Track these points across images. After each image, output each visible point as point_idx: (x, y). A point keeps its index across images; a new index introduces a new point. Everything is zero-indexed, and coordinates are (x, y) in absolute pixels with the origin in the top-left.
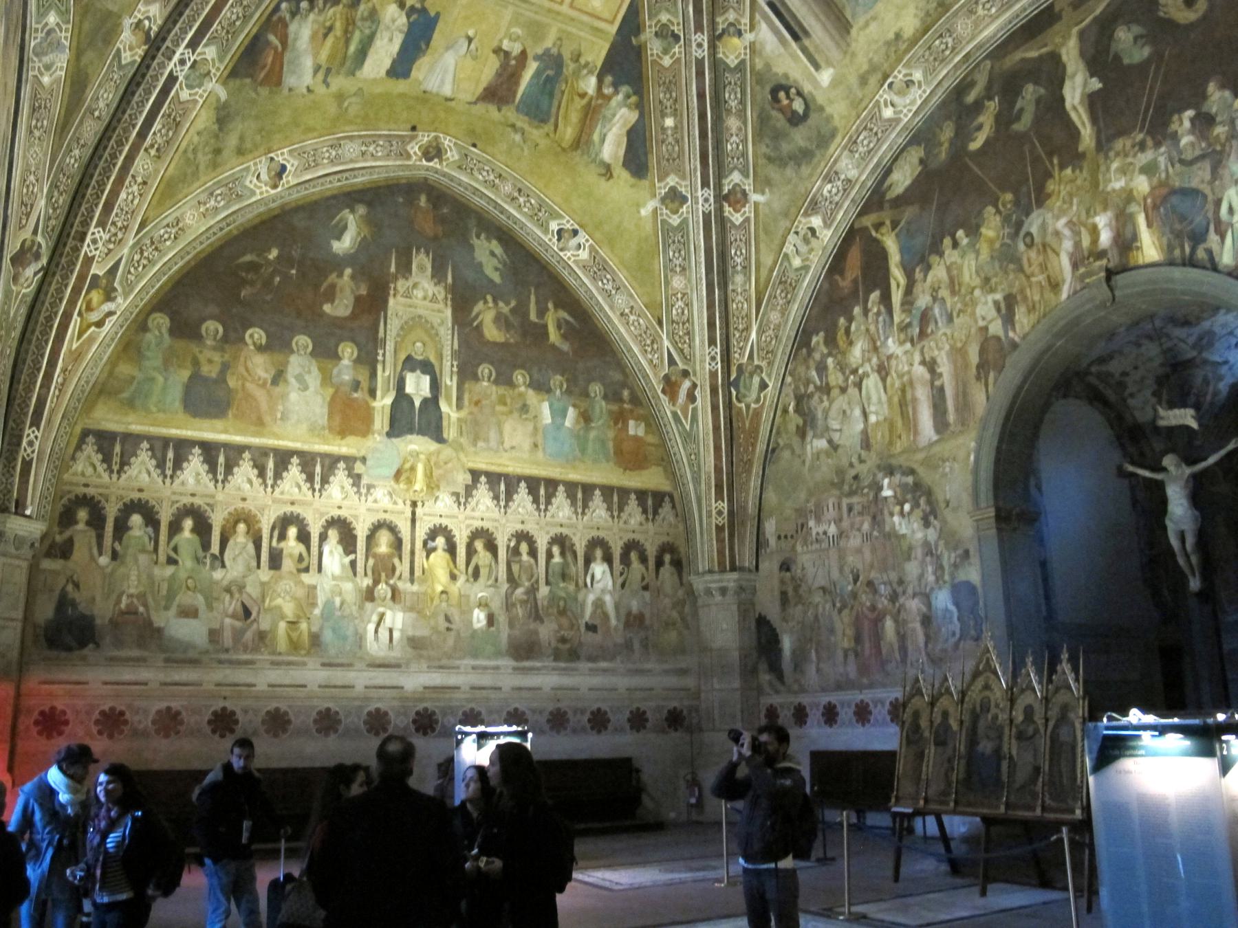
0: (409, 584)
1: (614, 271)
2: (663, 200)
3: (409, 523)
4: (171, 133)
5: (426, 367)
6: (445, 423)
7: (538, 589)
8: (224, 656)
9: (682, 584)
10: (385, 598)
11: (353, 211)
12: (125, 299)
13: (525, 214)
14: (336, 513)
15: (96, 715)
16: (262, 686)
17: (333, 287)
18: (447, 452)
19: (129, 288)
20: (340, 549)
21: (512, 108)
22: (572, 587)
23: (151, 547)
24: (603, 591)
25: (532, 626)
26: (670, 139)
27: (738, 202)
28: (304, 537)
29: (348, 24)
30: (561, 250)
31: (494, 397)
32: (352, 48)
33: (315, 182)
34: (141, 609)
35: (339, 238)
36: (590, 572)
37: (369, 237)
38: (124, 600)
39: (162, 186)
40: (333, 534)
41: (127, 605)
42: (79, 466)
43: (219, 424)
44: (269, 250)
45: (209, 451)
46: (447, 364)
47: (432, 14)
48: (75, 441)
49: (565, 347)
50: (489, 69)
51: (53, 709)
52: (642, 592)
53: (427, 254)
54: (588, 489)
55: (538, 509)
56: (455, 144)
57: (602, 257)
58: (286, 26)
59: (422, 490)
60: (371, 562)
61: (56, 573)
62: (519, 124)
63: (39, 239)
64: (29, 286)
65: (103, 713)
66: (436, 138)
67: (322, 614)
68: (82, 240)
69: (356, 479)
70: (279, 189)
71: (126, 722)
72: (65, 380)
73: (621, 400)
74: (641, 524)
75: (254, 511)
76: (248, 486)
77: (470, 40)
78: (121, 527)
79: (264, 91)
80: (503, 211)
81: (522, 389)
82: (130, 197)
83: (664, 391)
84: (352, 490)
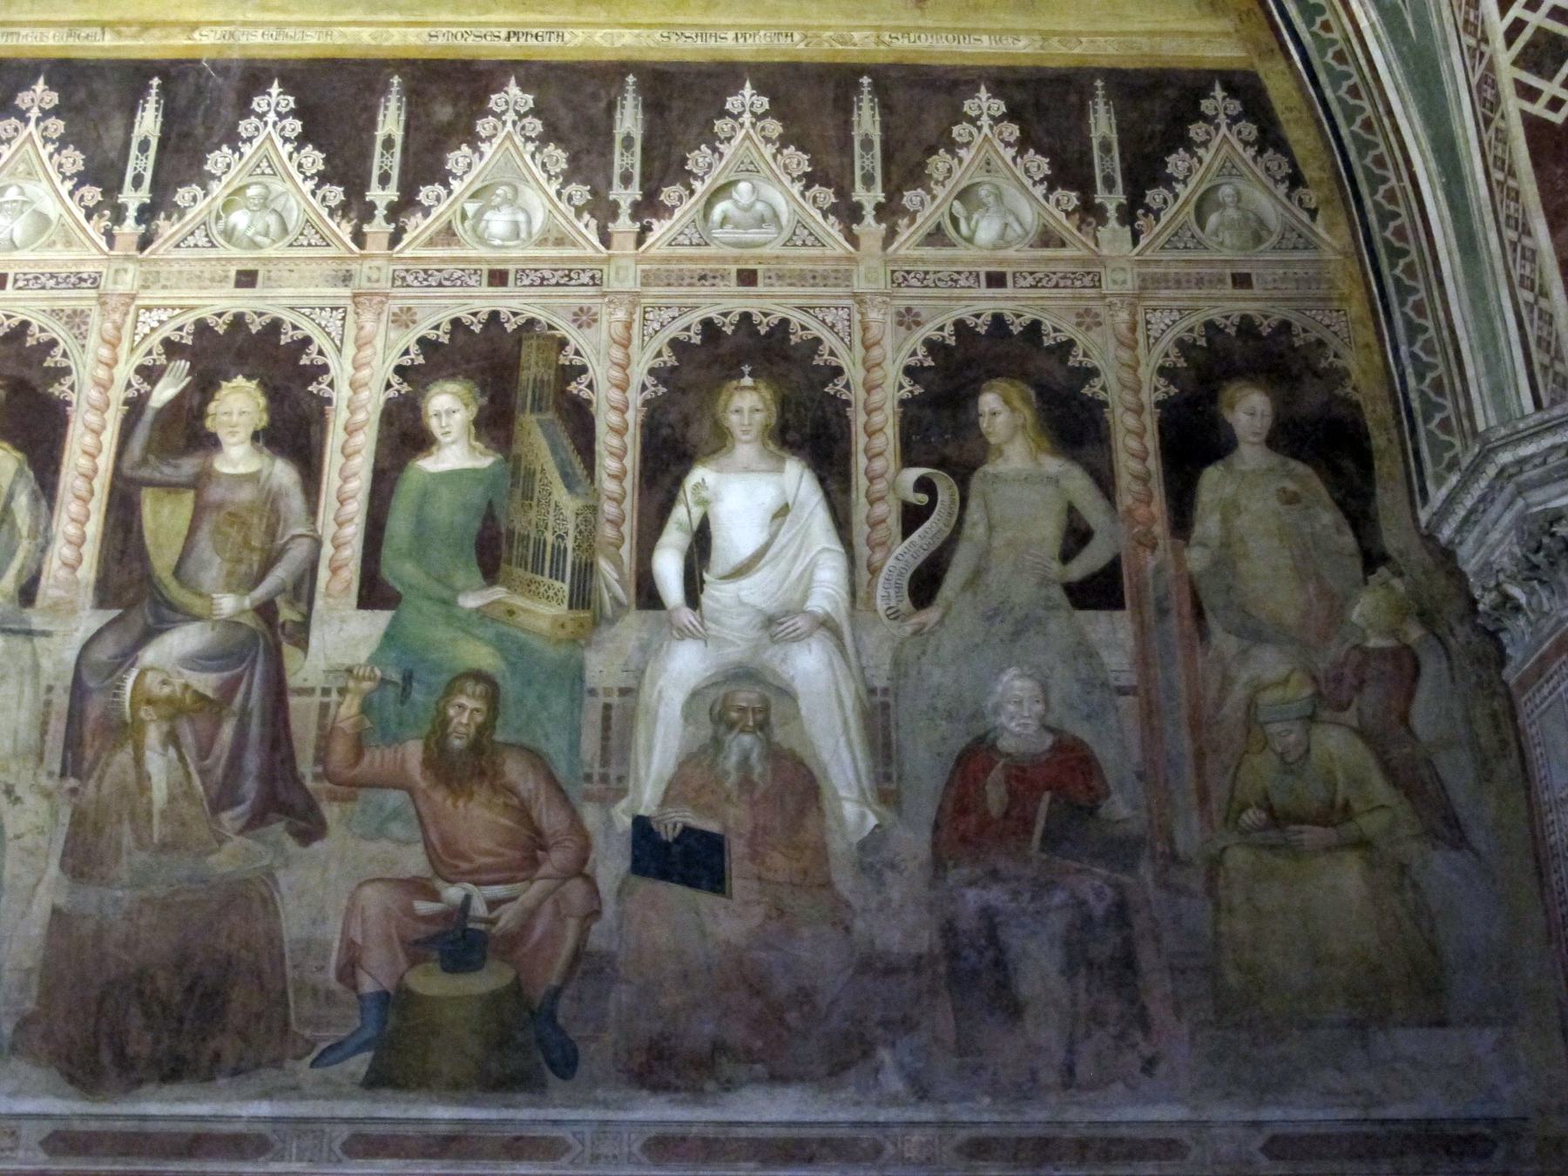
7: (301, 634)
9: (1372, 559)
36: (682, 516)
52: (1067, 623)
55: (356, 207)
74: (1047, 238)
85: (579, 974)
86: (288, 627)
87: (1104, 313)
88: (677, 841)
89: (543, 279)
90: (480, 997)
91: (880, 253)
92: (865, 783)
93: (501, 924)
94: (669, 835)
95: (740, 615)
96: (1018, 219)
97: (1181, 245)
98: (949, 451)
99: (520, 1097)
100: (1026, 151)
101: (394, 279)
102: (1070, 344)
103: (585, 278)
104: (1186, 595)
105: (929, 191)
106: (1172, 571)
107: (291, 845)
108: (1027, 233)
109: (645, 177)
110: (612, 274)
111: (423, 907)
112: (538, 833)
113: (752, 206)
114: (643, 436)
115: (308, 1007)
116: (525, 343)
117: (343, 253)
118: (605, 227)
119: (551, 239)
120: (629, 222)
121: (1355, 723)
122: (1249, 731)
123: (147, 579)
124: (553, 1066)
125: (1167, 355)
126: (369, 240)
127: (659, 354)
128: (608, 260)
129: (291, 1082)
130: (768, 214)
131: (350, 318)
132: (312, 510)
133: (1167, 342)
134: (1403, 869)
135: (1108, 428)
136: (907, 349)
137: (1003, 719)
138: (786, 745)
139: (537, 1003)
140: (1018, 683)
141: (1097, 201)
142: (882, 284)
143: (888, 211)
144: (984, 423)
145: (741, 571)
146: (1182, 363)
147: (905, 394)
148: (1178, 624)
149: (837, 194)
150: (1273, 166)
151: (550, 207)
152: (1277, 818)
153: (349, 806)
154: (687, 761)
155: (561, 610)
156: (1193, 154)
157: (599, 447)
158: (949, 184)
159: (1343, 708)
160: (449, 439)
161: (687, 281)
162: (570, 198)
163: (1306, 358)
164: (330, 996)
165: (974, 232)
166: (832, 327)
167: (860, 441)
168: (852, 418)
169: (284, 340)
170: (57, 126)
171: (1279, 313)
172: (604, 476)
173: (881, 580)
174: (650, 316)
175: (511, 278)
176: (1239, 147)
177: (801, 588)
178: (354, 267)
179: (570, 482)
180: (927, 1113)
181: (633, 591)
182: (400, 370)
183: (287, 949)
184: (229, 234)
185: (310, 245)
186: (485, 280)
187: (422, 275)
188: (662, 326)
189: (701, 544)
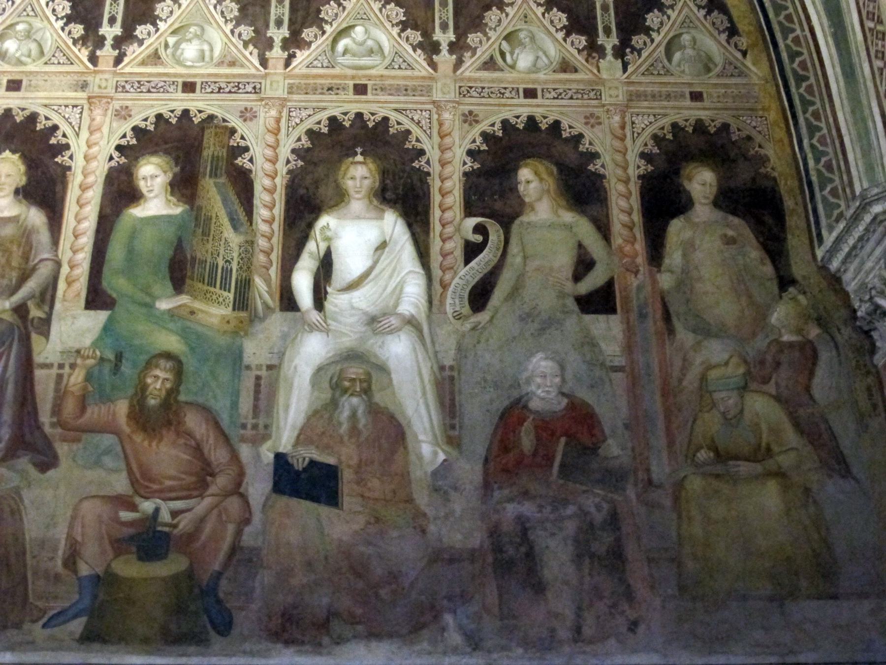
9: (785, 282)
36: (313, 248)
74: (565, 67)
85: (234, 562)
86: (36, 321)
87: (604, 117)
88: (305, 470)
89: (220, 88)
90: (163, 579)
91: (452, 74)
92: (438, 432)
93: (181, 526)
94: (299, 466)
95: (352, 315)
96: (545, 53)
97: (656, 73)
98: (498, 205)
99: (192, 649)
100: (552, 9)
101: (117, 87)
102: (581, 136)
103: (249, 88)
104: (658, 305)
105: (485, 34)
106: (649, 288)
107: (33, 472)
108: (552, 63)
109: (292, 22)
110: (268, 87)
111: (126, 515)
112: (207, 463)
113: (365, 41)
114: (287, 195)
115: (41, 582)
116: (207, 132)
117: (81, 69)
118: (264, 54)
119: (227, 61)
120: (280, 51)
121: (774, 393)
122: (701, 397)
124: (215, 627)
125: (646, 145)
126: (100, 60)
127: (299, 139)
128: (266, 75)
129: (30, 639)
130: (376, 48)
131: (85, 114)
132: (55, 241)
133: (646, 136)
134: (807, 491)
135: (606, 192)
136: (470, 137)
137: (533, 388)
138: (382, 405)
139: (205, 583)
140: (543, 363)
141: (599, 43)
142: (451, 96)
144: (521, 188)
146: (656, 150)
147: (467, 168)
148: (654, 323)
149: (422, 35)
150: (718, 22)
151: (227, 41)
152: (721, 456)
153: (75, 447)
154: (314, 415)
155: (226, 311)
156: (664, 13)
157: (256, 202)
158: (499, 29)
159: (766, 381)
160: (152, 195)
161: (320, 91)
162: (240, 35)
163: (740, 148)
164: (57, 578)
165: (515, 63)
166: (419, 123)
167: (436, 198)
168: (431, 183)
169: (39, 127)
171: (724, 117)
172: (260, 221)
173: (450, 293)
174: (293, 114)
175: (198, 87)
176: (695, 9)
177: (394, 297)
178: (90, 79)
179: (235, 225)
181: (277, 297)
182: (119, 148)
183: (28, 546)
185: (59, 63)
186: (180, 88)
187: (136, 85)
188: (301, 121)
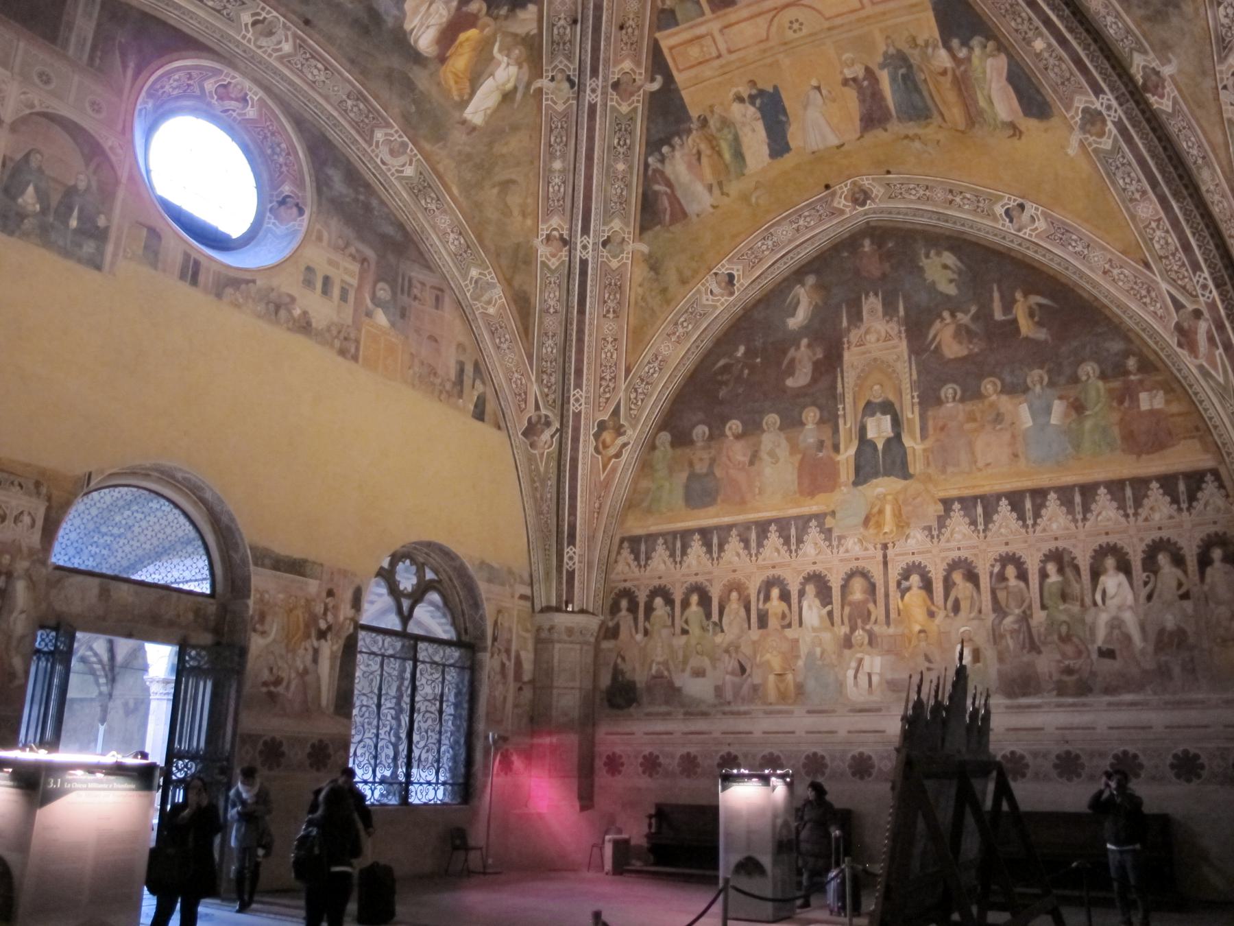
0: (885, 627)
1: (1076, 229)
2: (1083, 128)
3: (881, 566)
4: (618, 296)
5: (887, 407)
6: (910, 458)
7: (1031, 616)
8: (727, 709)
10: (862, 644)
11: (803, 285)
12: (634, 431)
13: (968, 212)
14: (811, 569)
15: (640, 760)
16: (758, 734)
17: (793, 361)
18: (913, 486)
19: (634, 420)
20: (817, 602)
21: (895, 120)
22: (1075, 608)
23: (669, 623)
24: (1120, 608)
25: (1026, 658)
26: (1052, 61)
27: (1156, 87)
28: (785, 597)
29: (710, 141)
30: (1019, 230)
31: (961, 417)
32: (727, 156)
33: (766, 274)
34: (666, 673)
35: (793, 315)
37: (820, 303)
38: (654, 668)
39: (630, 335)
40: (810, 589)
41: (657, 671)
42: (620, 567)
43: (712, 510)
44: (737, 350)
45: (705, 533)
46: (907, 398)
47: (771, 90)
48: (615, 548)
49: (1042, 335)
50: (852, 100)
51: (614, 754)
53: (876, 294)
54: (1088, 491)
55: (1025, 526)
56: (873, 179)
57: (1058, 220)
58: (662, 173)
59: (892, 531)
60: (847, 610)
61: (610, 650)
62: (911, 133)
63: (544, 412)
64: (551, 446)
65: (644, 757)
66: (854, 183)
67: (805, 665)
68: (569, 403)
69: (827, 533)
70: (736, 294)
71: (660, 765)
72: (600, 504)
73: (1127, 373)
74: (1171, 517)
75: (743, 580)
76: (737, 558)
77: (818, 88)
78: (649, 609)
79: (677, 228)
80: (947, 218)
81: (994, 397)
82: (609, 354)
83: (1180, 345)
84: (823, 544)
111: (1062, 665)
123: (1001, 608)
143: (1136, 514)
145: (1112, 598)
167: (1134, 568)
170: (962, 513)
179: (1077, 581)
180: (1157, 697)
184: (1001, 534)
189: (1104, 592)
